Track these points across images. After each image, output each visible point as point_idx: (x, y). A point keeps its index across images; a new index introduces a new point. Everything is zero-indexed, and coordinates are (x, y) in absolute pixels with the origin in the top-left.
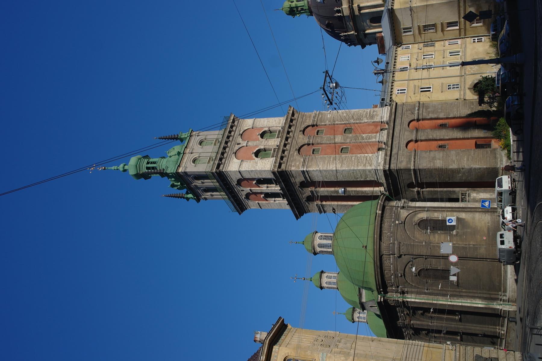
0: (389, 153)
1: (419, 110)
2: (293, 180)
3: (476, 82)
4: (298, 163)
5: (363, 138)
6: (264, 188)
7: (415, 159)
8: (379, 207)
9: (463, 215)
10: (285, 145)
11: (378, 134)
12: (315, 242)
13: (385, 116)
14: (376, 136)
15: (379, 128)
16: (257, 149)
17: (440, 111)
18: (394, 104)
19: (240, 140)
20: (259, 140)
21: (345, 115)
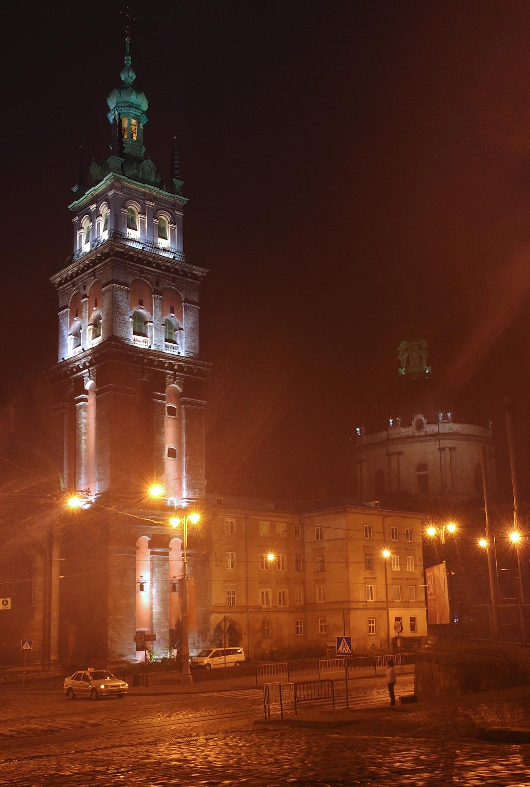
9: (39, 616)
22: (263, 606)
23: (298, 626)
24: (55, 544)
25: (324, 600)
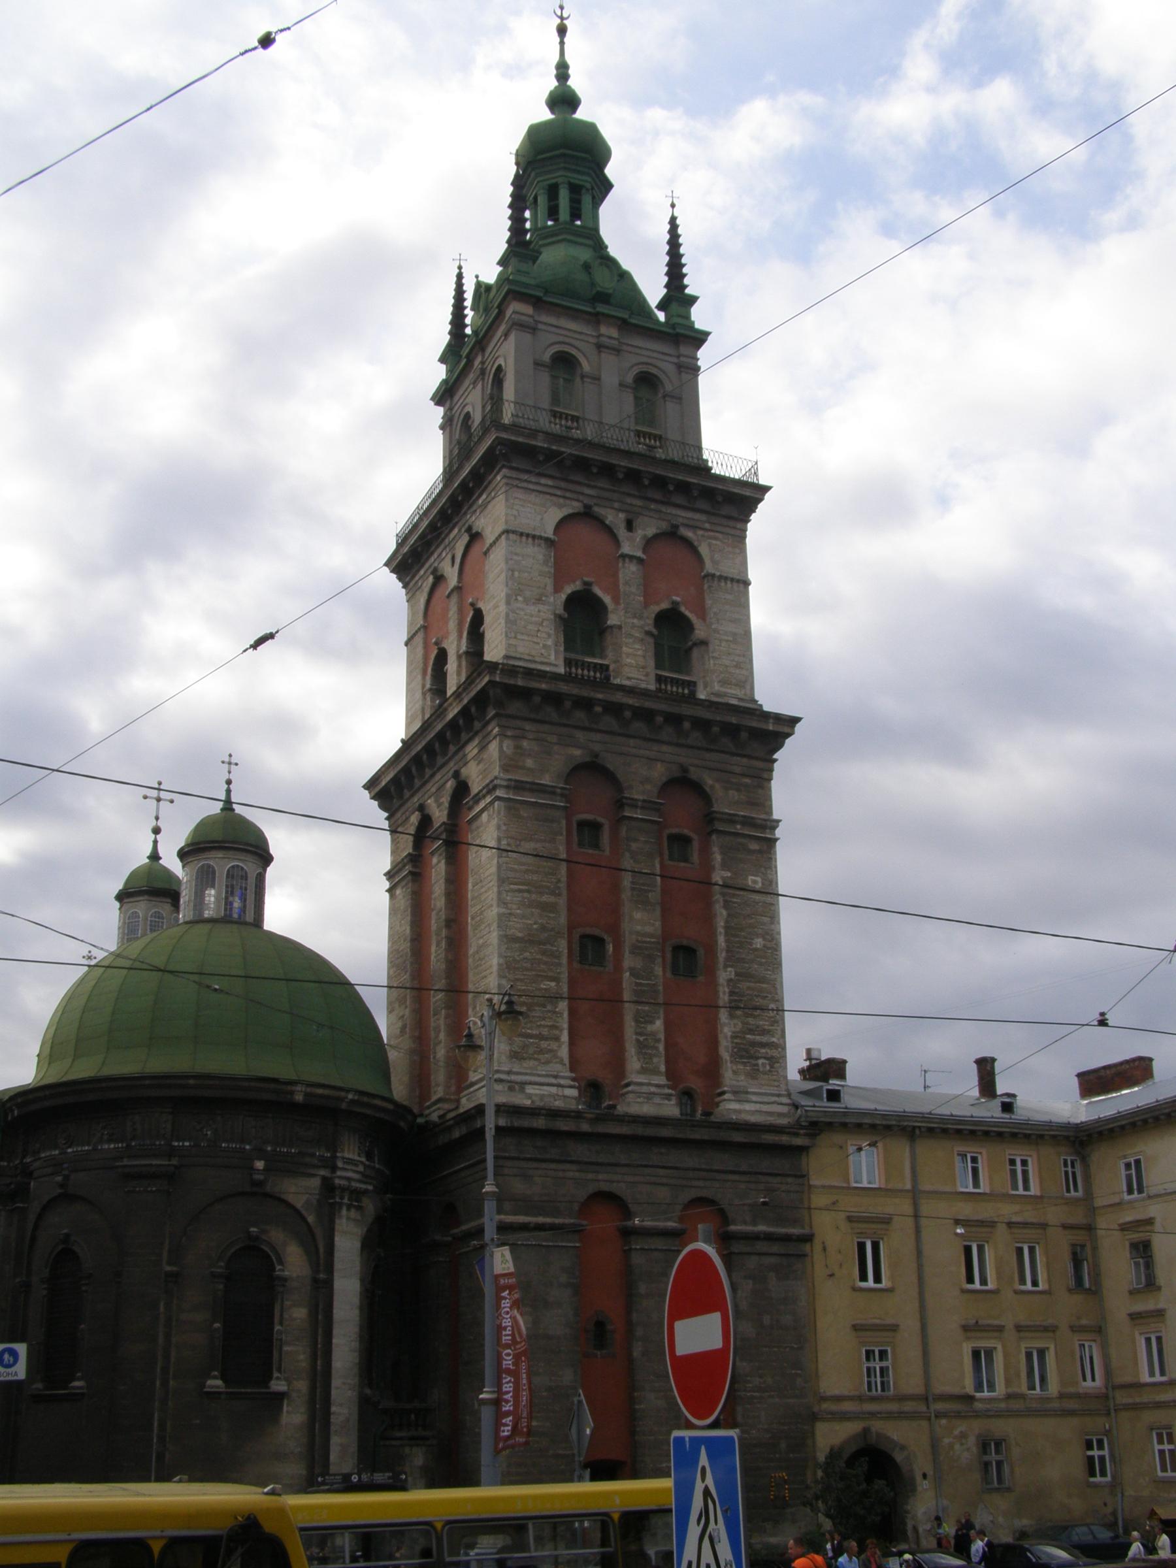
0: (563, 1125)
1: (769, 1238)
2: (471, 749)
3: (899, 1457)
4: (529, 763)
5: (642, 1020)
6: (455, 645)
7: (540, 1227)
8: (320, 1091)
9: (293, 1417)
10: (614, 709)
11: (662, 1080)
12: (220, 854)
13: (747, 1107)
14: (655, 1072)
15: (695, 1083)
16: (607, 599)
17: (767, 1320)
18: (798, 1141)
19: (648, 528)
20: (646, 605)
21: (759, 943)
22: (978, 1395)
23: (1090, 1453)
24: (344, 1212)
25: (1163, 1373)
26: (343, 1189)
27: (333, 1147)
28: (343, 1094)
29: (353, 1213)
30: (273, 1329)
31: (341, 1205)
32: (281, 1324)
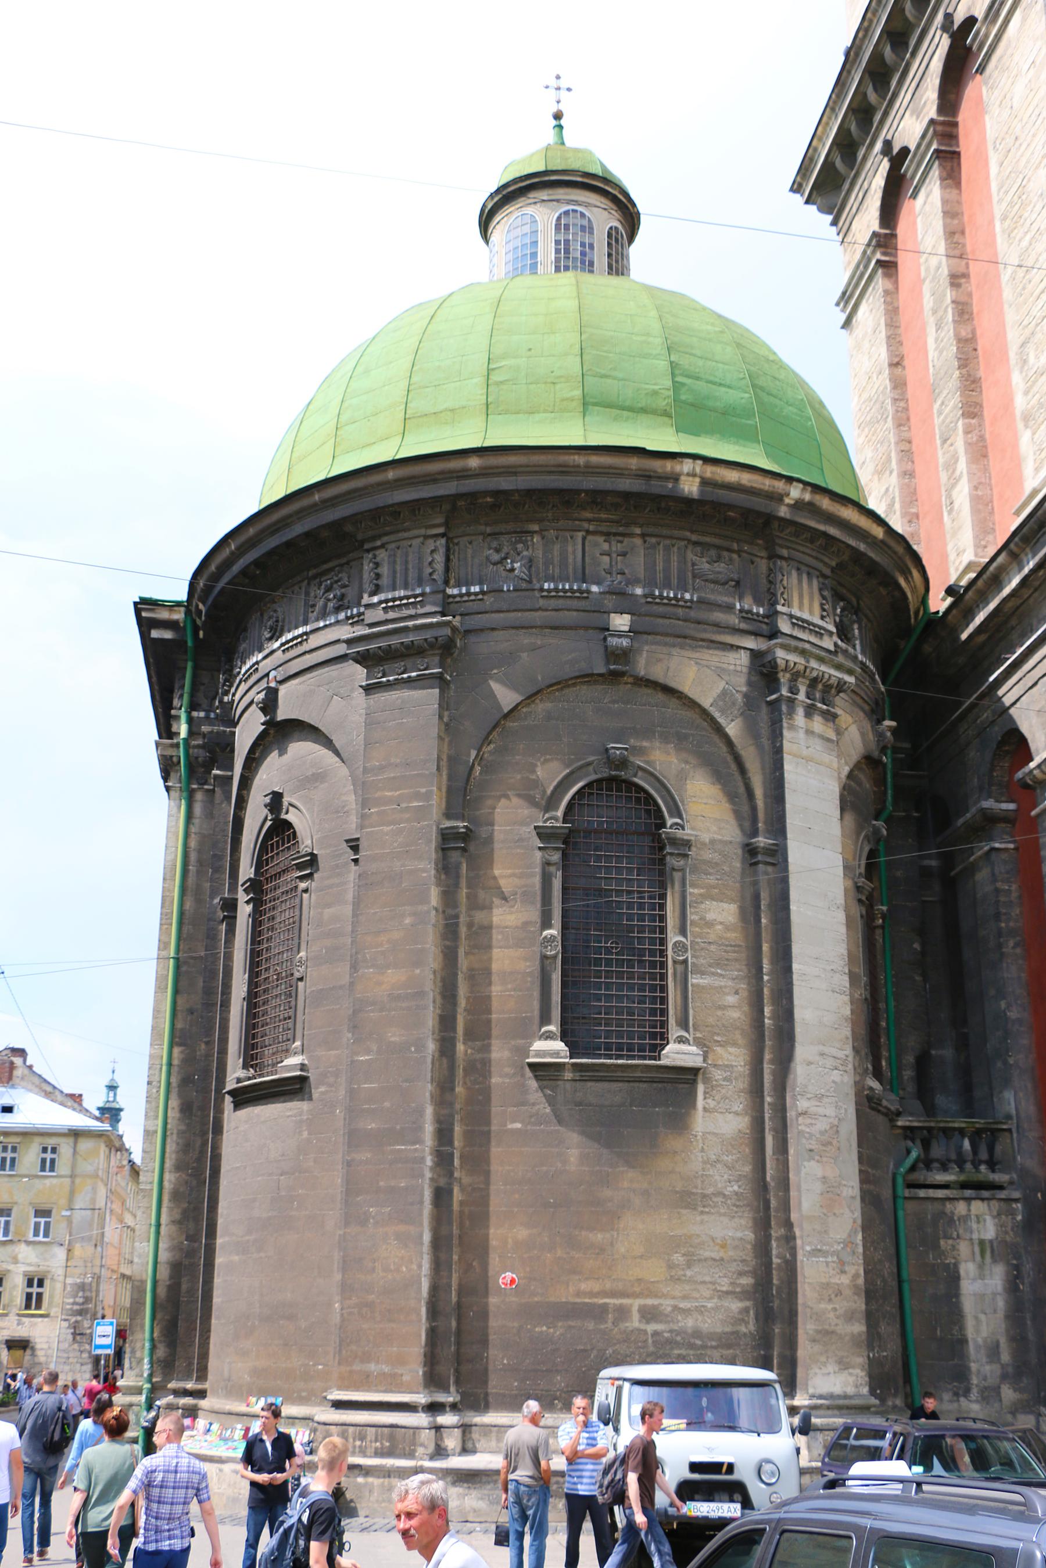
9: (718, 1119)
12: (544, 194)
26: (796, 676)
27: (770, 597)
28: (780, 485)
29: (818, 724)
30: (663, 942)
31: (791, 702)
32: (683, 931)
